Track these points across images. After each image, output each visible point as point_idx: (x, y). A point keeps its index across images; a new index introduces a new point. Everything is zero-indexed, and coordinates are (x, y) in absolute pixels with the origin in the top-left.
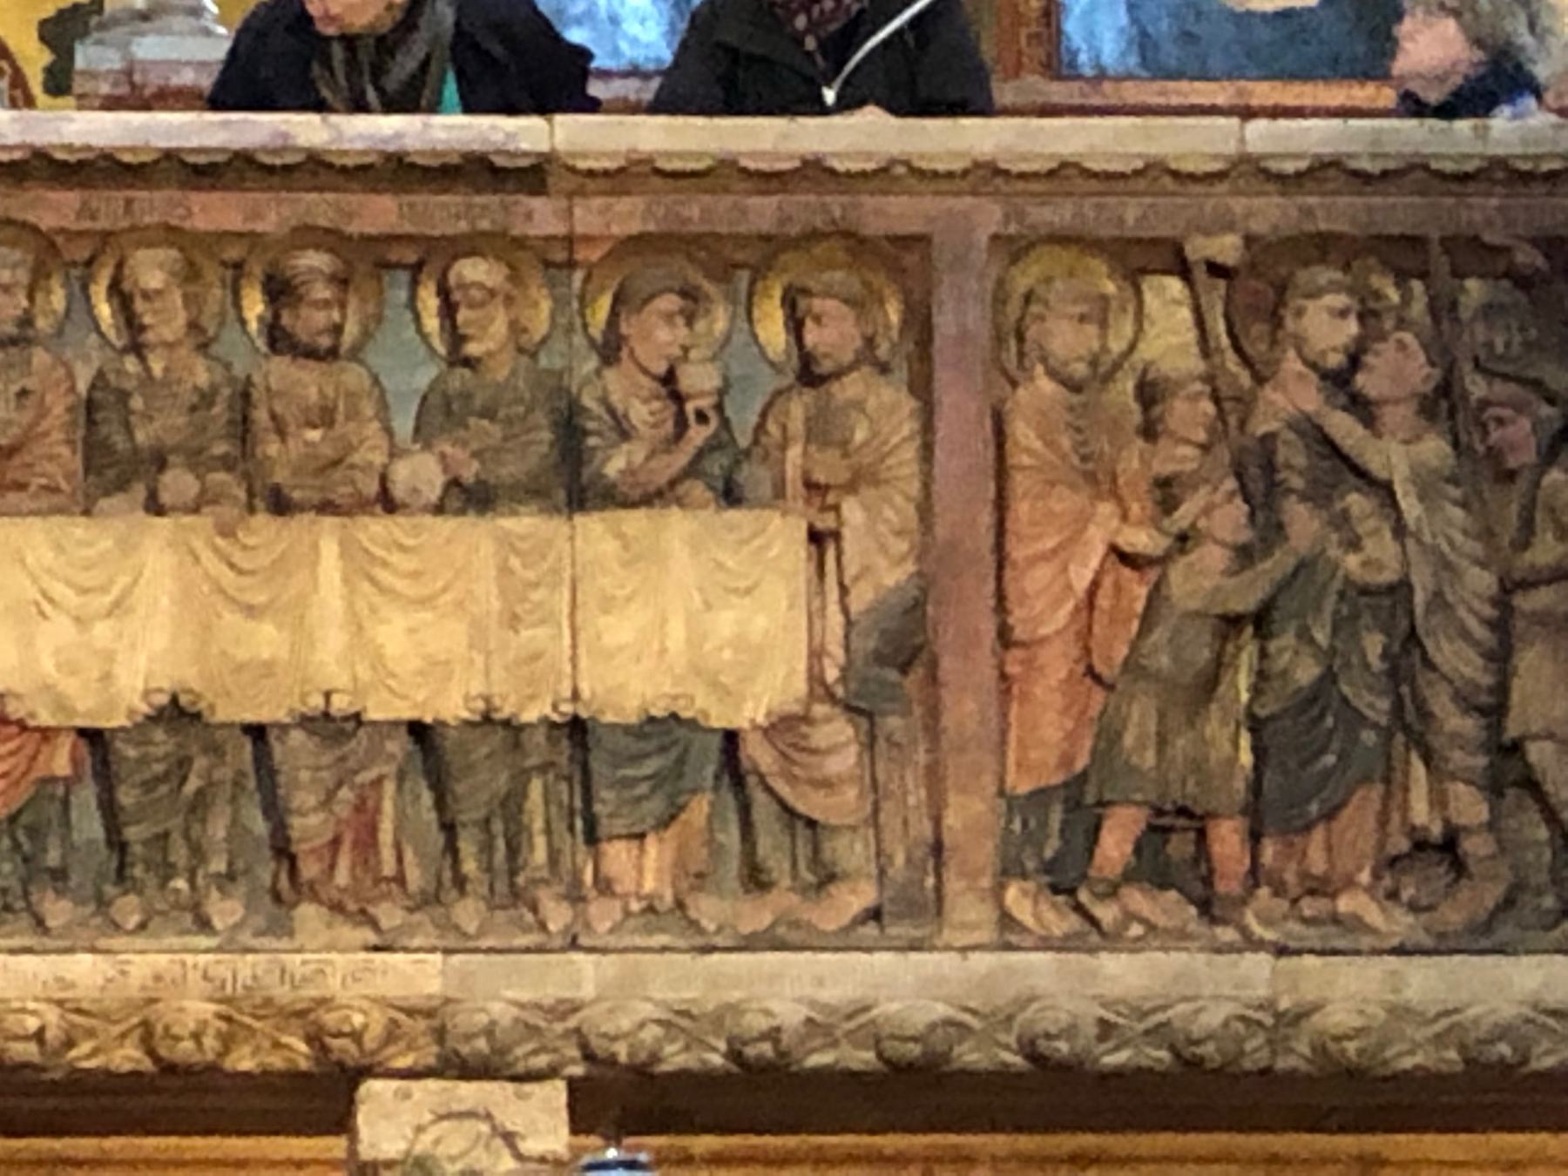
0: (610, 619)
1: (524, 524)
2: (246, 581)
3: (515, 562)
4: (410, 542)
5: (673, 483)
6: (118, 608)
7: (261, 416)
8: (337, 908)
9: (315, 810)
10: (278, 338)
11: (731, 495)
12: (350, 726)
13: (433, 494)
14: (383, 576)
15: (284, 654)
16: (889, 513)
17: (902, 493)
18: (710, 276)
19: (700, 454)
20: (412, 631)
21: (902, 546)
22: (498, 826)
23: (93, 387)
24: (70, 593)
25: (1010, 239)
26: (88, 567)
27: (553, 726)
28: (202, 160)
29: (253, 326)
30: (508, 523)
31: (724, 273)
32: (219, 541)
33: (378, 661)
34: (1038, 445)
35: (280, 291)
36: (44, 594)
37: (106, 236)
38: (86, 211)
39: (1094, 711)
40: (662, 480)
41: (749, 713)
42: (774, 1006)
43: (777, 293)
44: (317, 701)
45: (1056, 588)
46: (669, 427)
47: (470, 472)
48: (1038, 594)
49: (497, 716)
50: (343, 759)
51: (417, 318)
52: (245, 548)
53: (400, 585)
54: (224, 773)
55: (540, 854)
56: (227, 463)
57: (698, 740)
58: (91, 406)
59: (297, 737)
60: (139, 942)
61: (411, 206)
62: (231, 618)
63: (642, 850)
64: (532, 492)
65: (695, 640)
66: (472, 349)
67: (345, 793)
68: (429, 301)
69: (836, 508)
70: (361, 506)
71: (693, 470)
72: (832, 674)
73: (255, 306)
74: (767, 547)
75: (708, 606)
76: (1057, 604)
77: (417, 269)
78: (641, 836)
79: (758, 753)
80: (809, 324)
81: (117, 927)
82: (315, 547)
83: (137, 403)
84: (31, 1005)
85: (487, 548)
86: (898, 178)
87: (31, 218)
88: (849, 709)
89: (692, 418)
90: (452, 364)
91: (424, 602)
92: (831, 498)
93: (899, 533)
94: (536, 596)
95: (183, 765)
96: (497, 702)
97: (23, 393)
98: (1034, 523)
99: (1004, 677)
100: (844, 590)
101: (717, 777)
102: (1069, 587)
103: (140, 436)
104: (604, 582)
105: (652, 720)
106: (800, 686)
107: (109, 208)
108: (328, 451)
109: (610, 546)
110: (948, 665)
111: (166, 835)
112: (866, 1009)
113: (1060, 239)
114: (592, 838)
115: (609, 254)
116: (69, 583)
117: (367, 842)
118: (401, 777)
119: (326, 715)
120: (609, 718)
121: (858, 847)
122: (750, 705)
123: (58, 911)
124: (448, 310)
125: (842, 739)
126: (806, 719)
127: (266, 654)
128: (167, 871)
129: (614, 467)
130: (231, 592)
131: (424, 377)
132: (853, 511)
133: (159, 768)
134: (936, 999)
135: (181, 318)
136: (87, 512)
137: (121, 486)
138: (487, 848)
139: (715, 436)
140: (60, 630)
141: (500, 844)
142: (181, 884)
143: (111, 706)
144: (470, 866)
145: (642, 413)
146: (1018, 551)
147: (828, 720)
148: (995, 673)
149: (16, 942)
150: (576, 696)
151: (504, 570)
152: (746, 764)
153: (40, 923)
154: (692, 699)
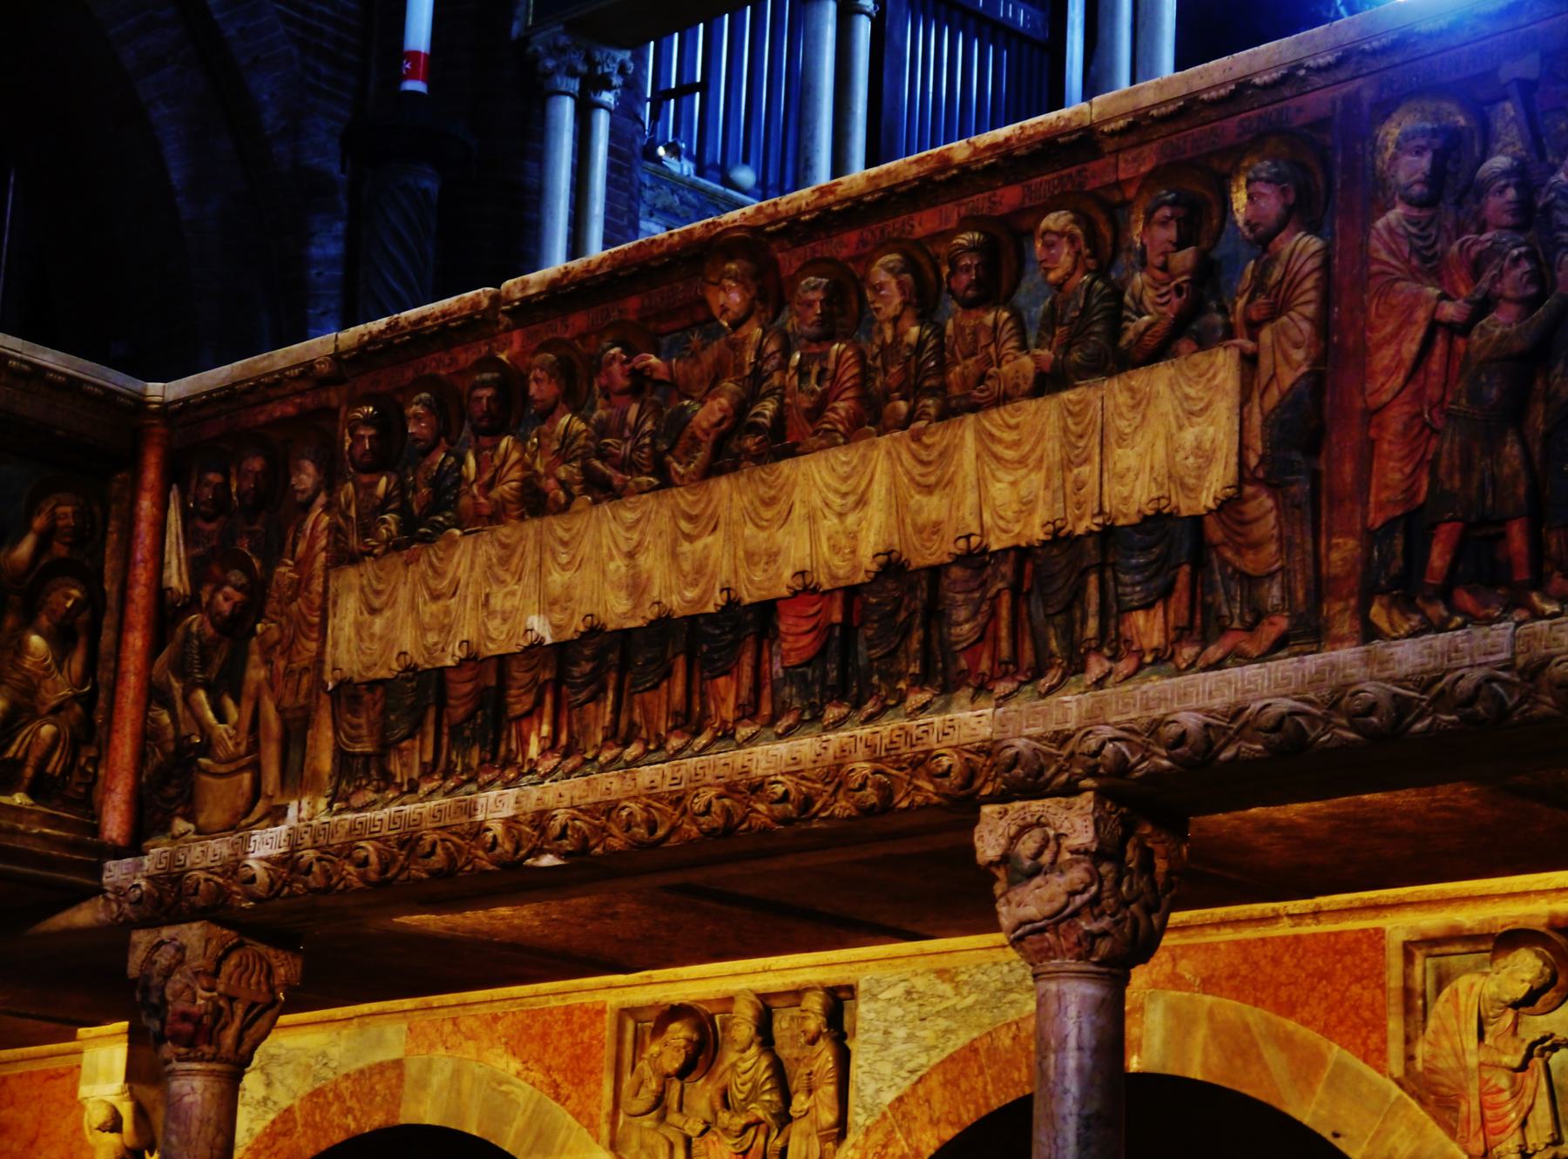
0: (1119, 451)
3: (1070, 421)
4: (1013, 421)
9: (967, 621)
14: (999, 449)
15: (944, 514)
17: (1301, 314)
26: (845, 479)
32: (914, 446)
34: (1384, 255)
42: (1182, 716)
44: (962, 543)
52: (927, 447)
53: (1009, 454)
59: (956, 572)
62: (918, 498)
65: (1170, 456)
72: (1253, 460)
75: (1181, 428)
79: (1215, 532)
84: (780, 778)
86: (1303, 79)
91: (1022, 462)
94: (1082, 444)
97: (823, 371)
104: (1122, 424)
105: (1146, 519)
109: (1123, 398)
112: (1243, 710)
116: (836, 491)
120: (1121, 522)
122: (1204, 494)
130: (918, 478)
134: (1286, 696)
147: (1255, 497)
150: (1101, 512)
151: (1065, 430)
154: (1169, 499)
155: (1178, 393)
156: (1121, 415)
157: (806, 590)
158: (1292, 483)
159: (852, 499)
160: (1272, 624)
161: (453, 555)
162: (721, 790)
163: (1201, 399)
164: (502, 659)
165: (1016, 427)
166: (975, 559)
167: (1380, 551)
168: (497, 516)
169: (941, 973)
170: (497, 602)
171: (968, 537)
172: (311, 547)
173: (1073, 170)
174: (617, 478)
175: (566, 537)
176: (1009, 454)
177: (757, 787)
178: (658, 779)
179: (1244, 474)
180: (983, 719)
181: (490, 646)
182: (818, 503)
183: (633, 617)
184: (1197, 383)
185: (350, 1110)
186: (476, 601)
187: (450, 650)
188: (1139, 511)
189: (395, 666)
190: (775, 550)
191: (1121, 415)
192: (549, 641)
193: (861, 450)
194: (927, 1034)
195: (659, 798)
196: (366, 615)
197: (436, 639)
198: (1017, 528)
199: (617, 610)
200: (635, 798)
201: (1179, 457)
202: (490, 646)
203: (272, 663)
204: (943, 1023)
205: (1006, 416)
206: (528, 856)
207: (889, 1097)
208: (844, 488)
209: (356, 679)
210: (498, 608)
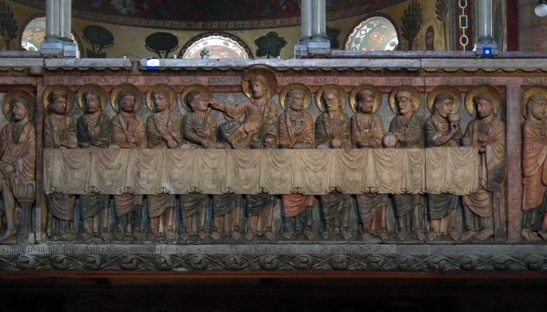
0: (433, 172)
1: (415, 150)
2: (351, 163)
4: (388, 154)
5: (447, 142)
6: (323, 169)
7: (355, 126)
8: (372, 235)
9: (367, 213)
10: (359, 109)
11: (461, 144)
12: (375, 195)
13: (393, 144)
14: (383, 162)
16: (497, 148)
17: (500, 143)
18: (456, 95)
19: (454, 135)
20: (389, 174)
21: (500, 155)
22: (408, 217)
23: (317, 121)
24: (313, 166)
25: (526, 86)
26: (316, 160)
27: (421, 195)
28: (342, 69)
29: (353, 107)
30: (410, 150)
31: (459, 94)
32: (346, 154)
33: (381, 181)
34: (531, 132)
35: (359, 98)
36: (306, 166)
37: (321, 86)
38: (315, 80)
39: (543, 192)
40: (446, 140)
41: (465, 192)
43: (471, 99)
44: (368, 189)
45: (535, 164)
46: (447, 129)
47: (402, 138)
48: (531, 166)
49: (408, 193)
50: (373, 202)
51: (390, 105)
53: (387, 164)
54: (347, 205)
55: (417, 223)
56: (347, 137)
57: (454, 198)
58: (317, 124)
59: (363, 197)
60: (329, 242)
61: (389, 80)
63: (440, 222)
64: (416, 143)
65: (454, 175)
66: (403, 111)
67: (373, 210)
68: (393, 100)
69: (485, 147)
70: (378, 147)
71: (451, 139)
72: (484, 183)
73: (353, 102)
74: (469, 155)
75: (456, 169)
76: (535, 168)
77: (390, 93)
78: (440, 219)
80: (479, 105)
81: (323, 239)
82: (367, 156)
83: (327, 124)
85: (406, 156)
87: (303, 83)
88: (487, 191)
89: (452, 126)
90: (397, 115)
91: (392, 168)
92: (484, 144)
93: (499, 152)
94: (418, 166)
95: (337, 204)
96: (408, 190)
98: (529, 150)
99: (523, 184)
100: (486, 165)
101: (458, 207)
102: (538, 164)
103: (328, 131)
105: (443, 193)
106: (476, 186)
107: (321, 80)
108: (370, 135)
110: (510, 182)
111: (334, 219)
113: (536, 86)
114: (429, 220)
115: (433, 90)
116: (312, 164)
117: (379, 220)
118: (386, 206)
119: (370, 193)
120: (433, 193)
121: (489, 222)
122: (465, 190)
123: (311, 236)
124: (397, 103)
125: (486, 198)
126: (477, 193)
127: (356, 179)
128: (334, 227)
129: (435, 138)
130: (349, 165)
131: (391, 118)
132: (489, 148)
133: (332, 204)
135: (337, 105)
136: (316, 148)
137: (323, 142)
138: (405, 222)
139: (458, 131)
140: (311, 174)
141: (408, 221)
142: (337, 229)
143: (322, 190)
144: (402, 225)
145: (441, 125)
146: (527, 156)
147: (483, 194)
148: (520, 184)
149: (301, 242)
150: (426, 189)
151: (410, 161)
152: (464, 204)
153: (306, 238)
154: (452, 189)
155: (455, 158)
156: (433, 160)
157: (297, 194)
158: (497, 192)
159: (320, 168)
160: (488, 231)
161: (118, 154)
162: (277, 256)
163: (465, 162)
164: (145, 197)
165: (390, 156)
166: (371, 195)
167: (527, 216)
168: (137, 144)
170: (143, 175)
171: (370, 188)
172: (28, 138)
173: (407, 78)
174: (204, 142)
175: (180, 158)
176: (387, 164)
177: (293, 258)
178: (248, 249)
179: (481, 187)
180: (393, 247)
181: (142, 190)
182: (304, 166)
183: (216, 191)
184: (463, 157)
186: (133, 172)
187: (119, 188)
188: (441, 191)
189: (87, 190)
190: (285, 178)
191: (433, 160)
192: (172, 192)
193: (324, 152)
195: (248, 256)
196: (69, 169)
197: (111, 184)
198: (391, 188)
199: (209, 187)
200: (237, 255)
201: (457, 177)
202: (142, 190)
203: (9, 180)
205: (385, 152)
206: (174, 268)
208: (315, 163)
209: (65, 192)
210: (145, 178)
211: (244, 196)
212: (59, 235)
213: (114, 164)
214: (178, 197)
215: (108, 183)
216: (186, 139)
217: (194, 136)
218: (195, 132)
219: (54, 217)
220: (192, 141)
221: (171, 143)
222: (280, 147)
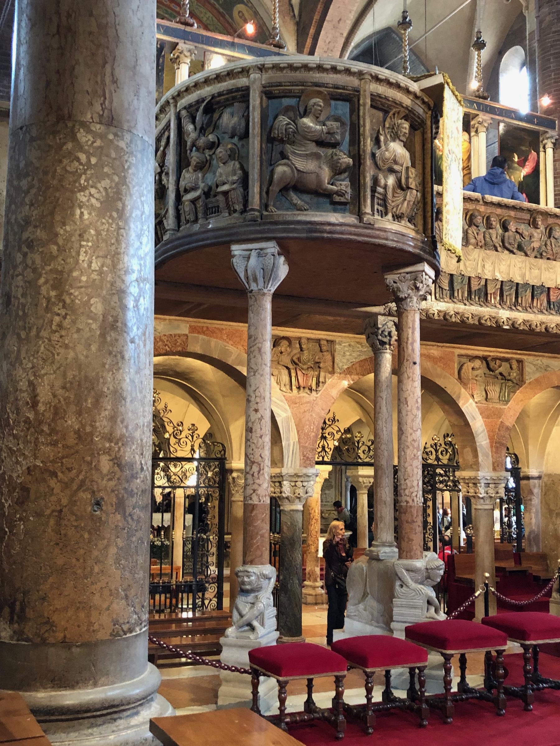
164: (486, 280)
168: (481, 247)
169: (358, 342)
174: (515, 251)
185: (166, 345)
194: (355, 354)
199: (518, 279)
204: (358, 353)
207: (345, 367)
211: (533, 286)
212: (443, 298)
213: (471, 258)
214: (502, 282)
215: (469, 269)
216: (505, 247)
217: (509, 247)
218: (510, 244)
219: (439, 287)
220: (508, 250)
221: (499, 249)
222: (548, 259)
